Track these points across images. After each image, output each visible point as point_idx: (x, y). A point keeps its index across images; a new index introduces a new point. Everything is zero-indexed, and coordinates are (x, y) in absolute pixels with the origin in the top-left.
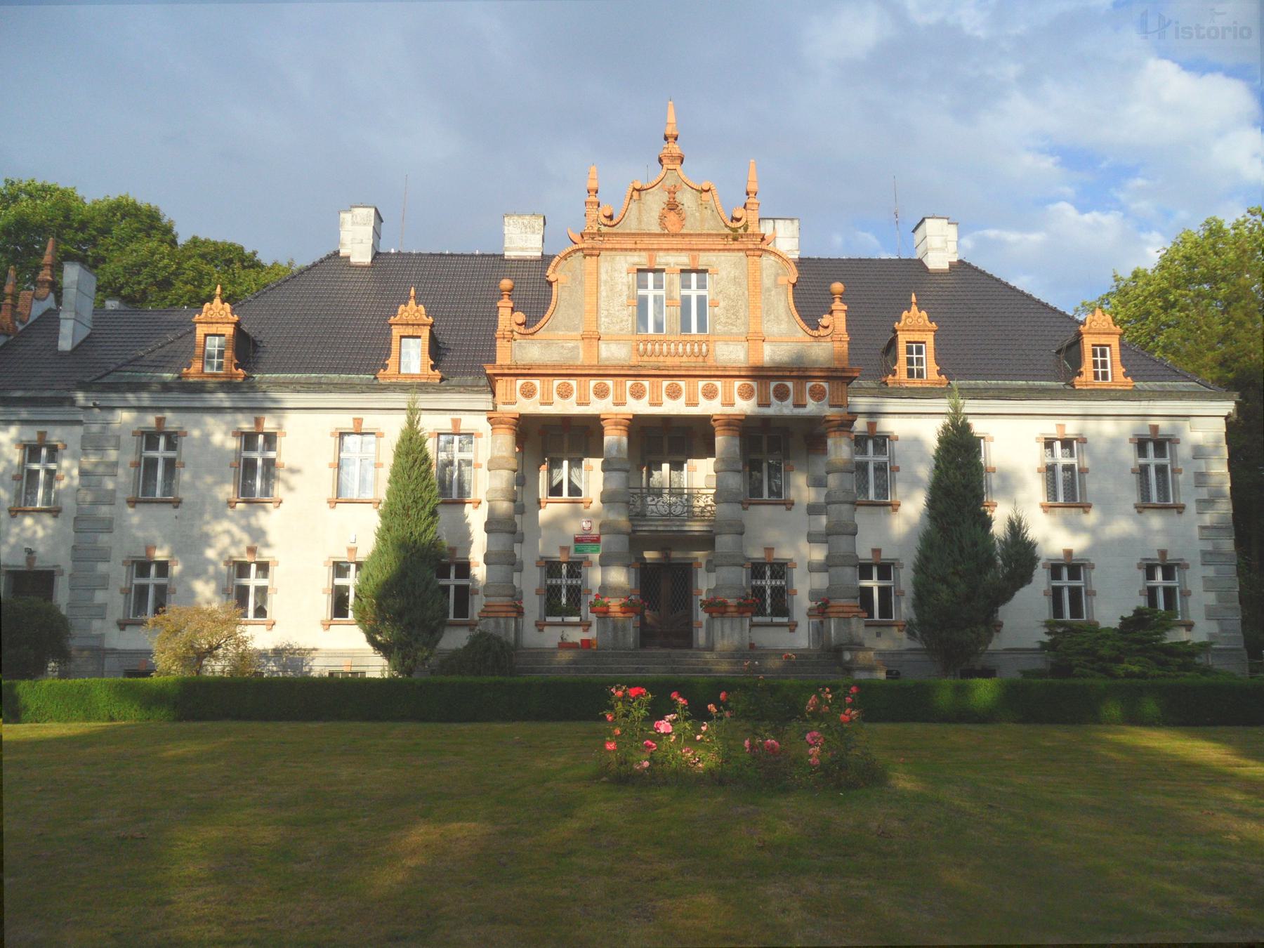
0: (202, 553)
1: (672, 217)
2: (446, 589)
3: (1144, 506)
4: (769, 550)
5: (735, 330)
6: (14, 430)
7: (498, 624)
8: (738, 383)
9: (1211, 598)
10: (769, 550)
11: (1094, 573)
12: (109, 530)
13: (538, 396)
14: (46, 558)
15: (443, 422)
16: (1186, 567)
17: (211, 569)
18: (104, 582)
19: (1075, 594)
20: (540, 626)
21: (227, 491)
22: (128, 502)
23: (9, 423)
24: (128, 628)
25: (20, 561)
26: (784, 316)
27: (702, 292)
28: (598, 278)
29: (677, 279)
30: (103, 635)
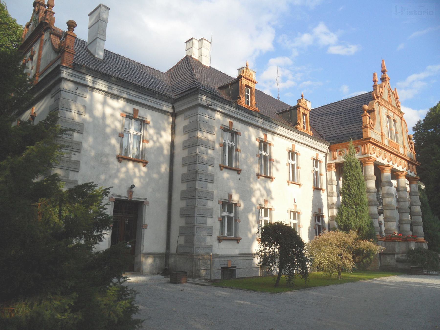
0: (250, 200)
6: (120, 104)
8: (403, 162)
12: (212, 182)
17: (254, 209)
21: (256, 169)
22: (220, 166)
23: (116, 97)
24: (223, 242)
25: (123, 193)
30: (212, 246)
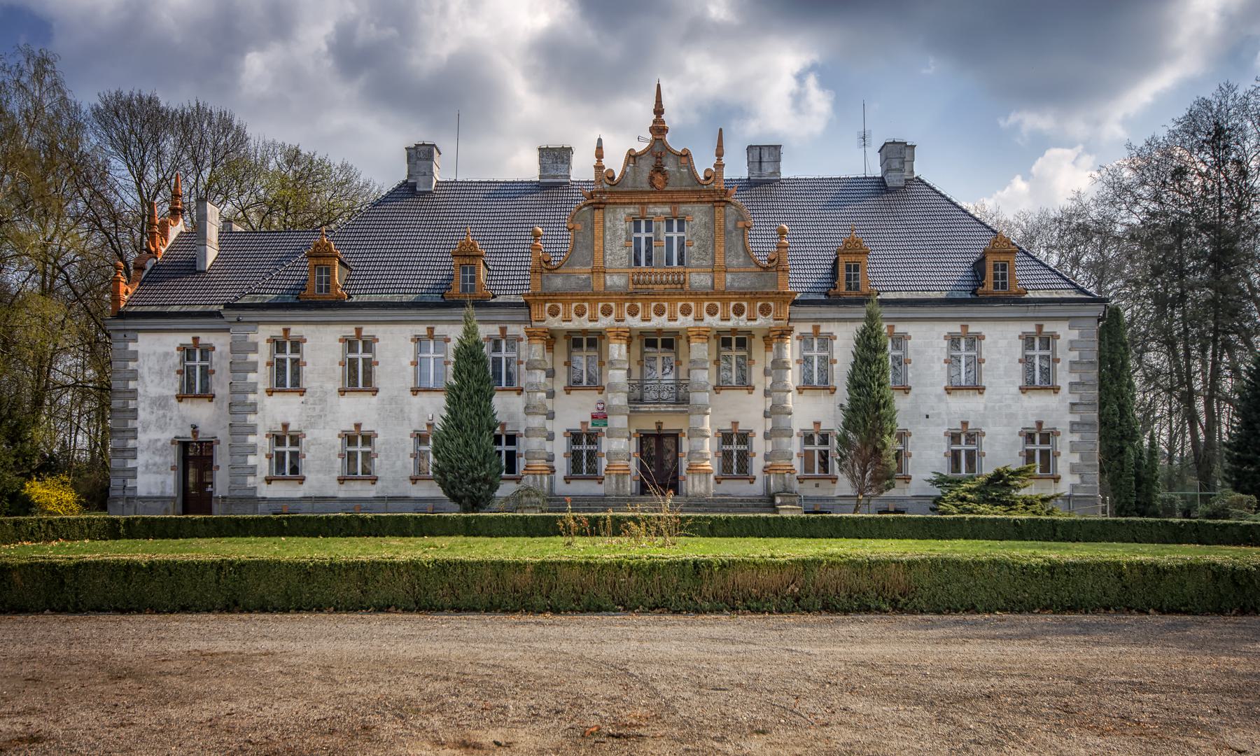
1: (659, 177)
2: (500, 453)
3: (1028, 387)
4: (735, 424)
5: (705, 263)
7: (535, 479)
9: (1076, 458)
10: (735, 424)
11: (984, 439)
12: (255, 412)
13: (560, 315)
14: (205, 432)
15: (494, 330)
16: (1058, 434)
18: (253, 450)
19: (971, 456)
20: (567, 480)
25: (187, 433)
26: (741, 252)
27: (681, 234)
28: (604, 226)
29: (663, 226)
